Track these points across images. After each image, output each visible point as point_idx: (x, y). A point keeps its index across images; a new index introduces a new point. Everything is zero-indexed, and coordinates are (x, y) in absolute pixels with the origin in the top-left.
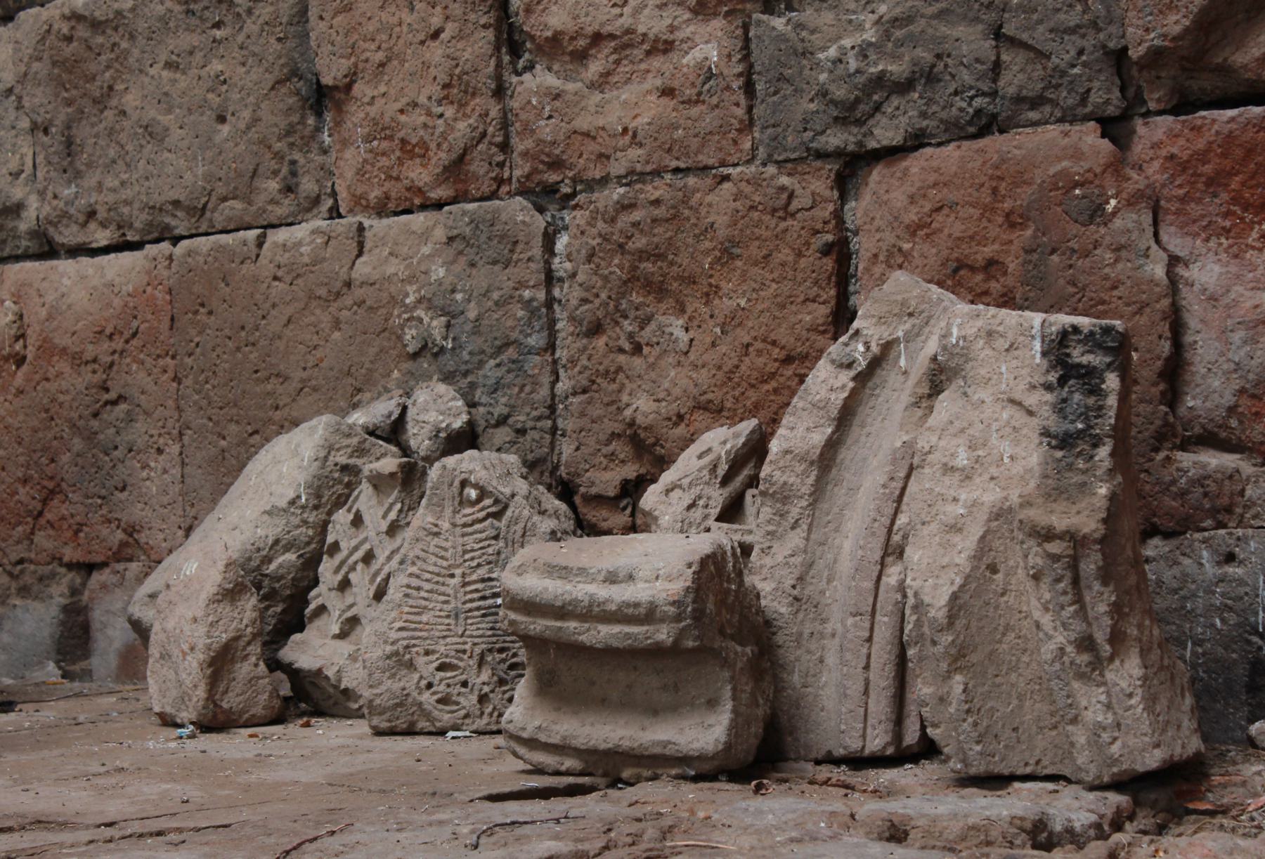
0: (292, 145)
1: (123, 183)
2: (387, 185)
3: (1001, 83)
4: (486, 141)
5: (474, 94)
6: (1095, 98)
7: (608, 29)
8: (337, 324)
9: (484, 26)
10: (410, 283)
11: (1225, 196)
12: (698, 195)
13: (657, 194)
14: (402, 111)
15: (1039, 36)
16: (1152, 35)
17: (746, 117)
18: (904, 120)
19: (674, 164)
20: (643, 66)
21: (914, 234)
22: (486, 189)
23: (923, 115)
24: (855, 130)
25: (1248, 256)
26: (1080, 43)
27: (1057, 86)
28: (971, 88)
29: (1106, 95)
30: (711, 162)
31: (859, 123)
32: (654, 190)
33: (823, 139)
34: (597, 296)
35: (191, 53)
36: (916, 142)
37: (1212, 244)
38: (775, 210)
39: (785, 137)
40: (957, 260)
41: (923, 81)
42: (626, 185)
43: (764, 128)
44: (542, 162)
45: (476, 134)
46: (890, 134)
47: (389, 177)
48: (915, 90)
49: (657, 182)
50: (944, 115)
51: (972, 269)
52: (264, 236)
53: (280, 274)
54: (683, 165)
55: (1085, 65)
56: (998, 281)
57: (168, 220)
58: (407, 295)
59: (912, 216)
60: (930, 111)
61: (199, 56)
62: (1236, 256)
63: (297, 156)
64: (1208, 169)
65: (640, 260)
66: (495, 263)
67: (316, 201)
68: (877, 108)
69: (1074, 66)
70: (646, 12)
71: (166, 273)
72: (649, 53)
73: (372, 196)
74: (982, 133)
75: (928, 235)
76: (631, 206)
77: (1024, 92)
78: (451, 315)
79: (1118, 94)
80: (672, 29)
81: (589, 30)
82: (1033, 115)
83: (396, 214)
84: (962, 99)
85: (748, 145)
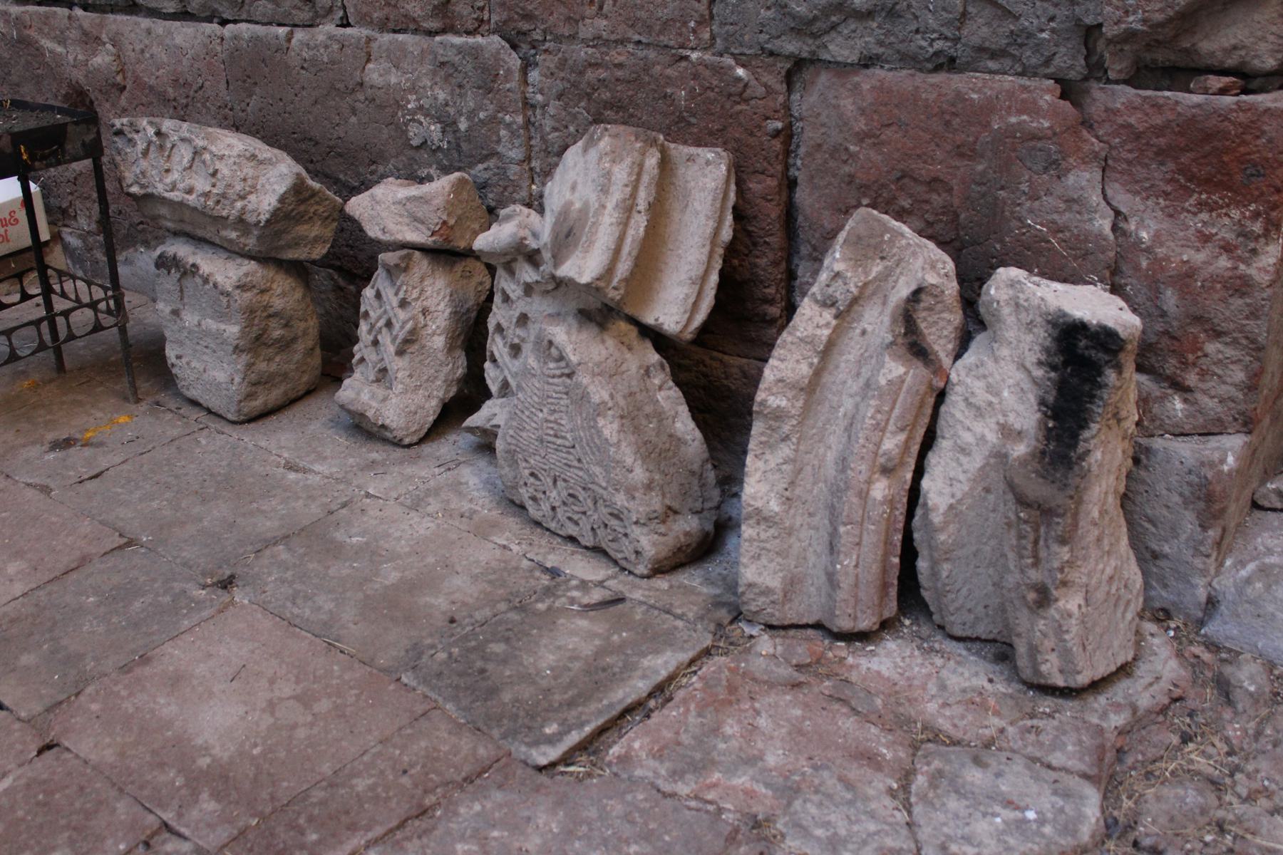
2: (387, 10)
3: (965, 32)
6: (1057, 61)
8: (354, 111)
10: (410, 93)
11: (1171, 165)
12: (658, 68)
13: (621, 59)
16: (1131, 19)
17: (706, 13)
18: (859, 43)
19: (637, 37)
21: (862, 140)
22: (470, 25)
23: (881, 43)
24: (810, 41)
25: (1182, 217)
27: (1021, 46)
28: (934, 31)
29: (1069, 60)
30: (672, 43)
31: (814, 36)
32: (617, 55)
33: (778, 42)
34: (566, 127)
36: (867, 62)
37: (1149, 203)
38: (730, 95)
39: (742, 35)
40: (903, 171)
41: (883, 14)
42: (593, 47)
43: (723, 24)
44: (517, 13)
46: (846, 53)
48: (873, 20)
49: (620, 49)
50: (902, 47)
52: (292, 33)
54: (644, 40)
55: (1053, 31)
56: (939, 195)
58: (409, 102)
59: (861, 125)
60: (887, 41)
62: (1171, 216)
64: (1162, 141)
65: (605, 108)
66: (479, 88)
67: (330, 10)
68: (834, 27)
69: (1042, 31)
71: (219, 48)
73: (375, 15)
74: (937, 69)
75: (874, 144)
76: (596, 65)
77: (987, 44)
78: (448, 125)
79: (1083, 62)
82: (992, 65)
83: (395, 32)
84: (923, 39)
85: (707, 36)
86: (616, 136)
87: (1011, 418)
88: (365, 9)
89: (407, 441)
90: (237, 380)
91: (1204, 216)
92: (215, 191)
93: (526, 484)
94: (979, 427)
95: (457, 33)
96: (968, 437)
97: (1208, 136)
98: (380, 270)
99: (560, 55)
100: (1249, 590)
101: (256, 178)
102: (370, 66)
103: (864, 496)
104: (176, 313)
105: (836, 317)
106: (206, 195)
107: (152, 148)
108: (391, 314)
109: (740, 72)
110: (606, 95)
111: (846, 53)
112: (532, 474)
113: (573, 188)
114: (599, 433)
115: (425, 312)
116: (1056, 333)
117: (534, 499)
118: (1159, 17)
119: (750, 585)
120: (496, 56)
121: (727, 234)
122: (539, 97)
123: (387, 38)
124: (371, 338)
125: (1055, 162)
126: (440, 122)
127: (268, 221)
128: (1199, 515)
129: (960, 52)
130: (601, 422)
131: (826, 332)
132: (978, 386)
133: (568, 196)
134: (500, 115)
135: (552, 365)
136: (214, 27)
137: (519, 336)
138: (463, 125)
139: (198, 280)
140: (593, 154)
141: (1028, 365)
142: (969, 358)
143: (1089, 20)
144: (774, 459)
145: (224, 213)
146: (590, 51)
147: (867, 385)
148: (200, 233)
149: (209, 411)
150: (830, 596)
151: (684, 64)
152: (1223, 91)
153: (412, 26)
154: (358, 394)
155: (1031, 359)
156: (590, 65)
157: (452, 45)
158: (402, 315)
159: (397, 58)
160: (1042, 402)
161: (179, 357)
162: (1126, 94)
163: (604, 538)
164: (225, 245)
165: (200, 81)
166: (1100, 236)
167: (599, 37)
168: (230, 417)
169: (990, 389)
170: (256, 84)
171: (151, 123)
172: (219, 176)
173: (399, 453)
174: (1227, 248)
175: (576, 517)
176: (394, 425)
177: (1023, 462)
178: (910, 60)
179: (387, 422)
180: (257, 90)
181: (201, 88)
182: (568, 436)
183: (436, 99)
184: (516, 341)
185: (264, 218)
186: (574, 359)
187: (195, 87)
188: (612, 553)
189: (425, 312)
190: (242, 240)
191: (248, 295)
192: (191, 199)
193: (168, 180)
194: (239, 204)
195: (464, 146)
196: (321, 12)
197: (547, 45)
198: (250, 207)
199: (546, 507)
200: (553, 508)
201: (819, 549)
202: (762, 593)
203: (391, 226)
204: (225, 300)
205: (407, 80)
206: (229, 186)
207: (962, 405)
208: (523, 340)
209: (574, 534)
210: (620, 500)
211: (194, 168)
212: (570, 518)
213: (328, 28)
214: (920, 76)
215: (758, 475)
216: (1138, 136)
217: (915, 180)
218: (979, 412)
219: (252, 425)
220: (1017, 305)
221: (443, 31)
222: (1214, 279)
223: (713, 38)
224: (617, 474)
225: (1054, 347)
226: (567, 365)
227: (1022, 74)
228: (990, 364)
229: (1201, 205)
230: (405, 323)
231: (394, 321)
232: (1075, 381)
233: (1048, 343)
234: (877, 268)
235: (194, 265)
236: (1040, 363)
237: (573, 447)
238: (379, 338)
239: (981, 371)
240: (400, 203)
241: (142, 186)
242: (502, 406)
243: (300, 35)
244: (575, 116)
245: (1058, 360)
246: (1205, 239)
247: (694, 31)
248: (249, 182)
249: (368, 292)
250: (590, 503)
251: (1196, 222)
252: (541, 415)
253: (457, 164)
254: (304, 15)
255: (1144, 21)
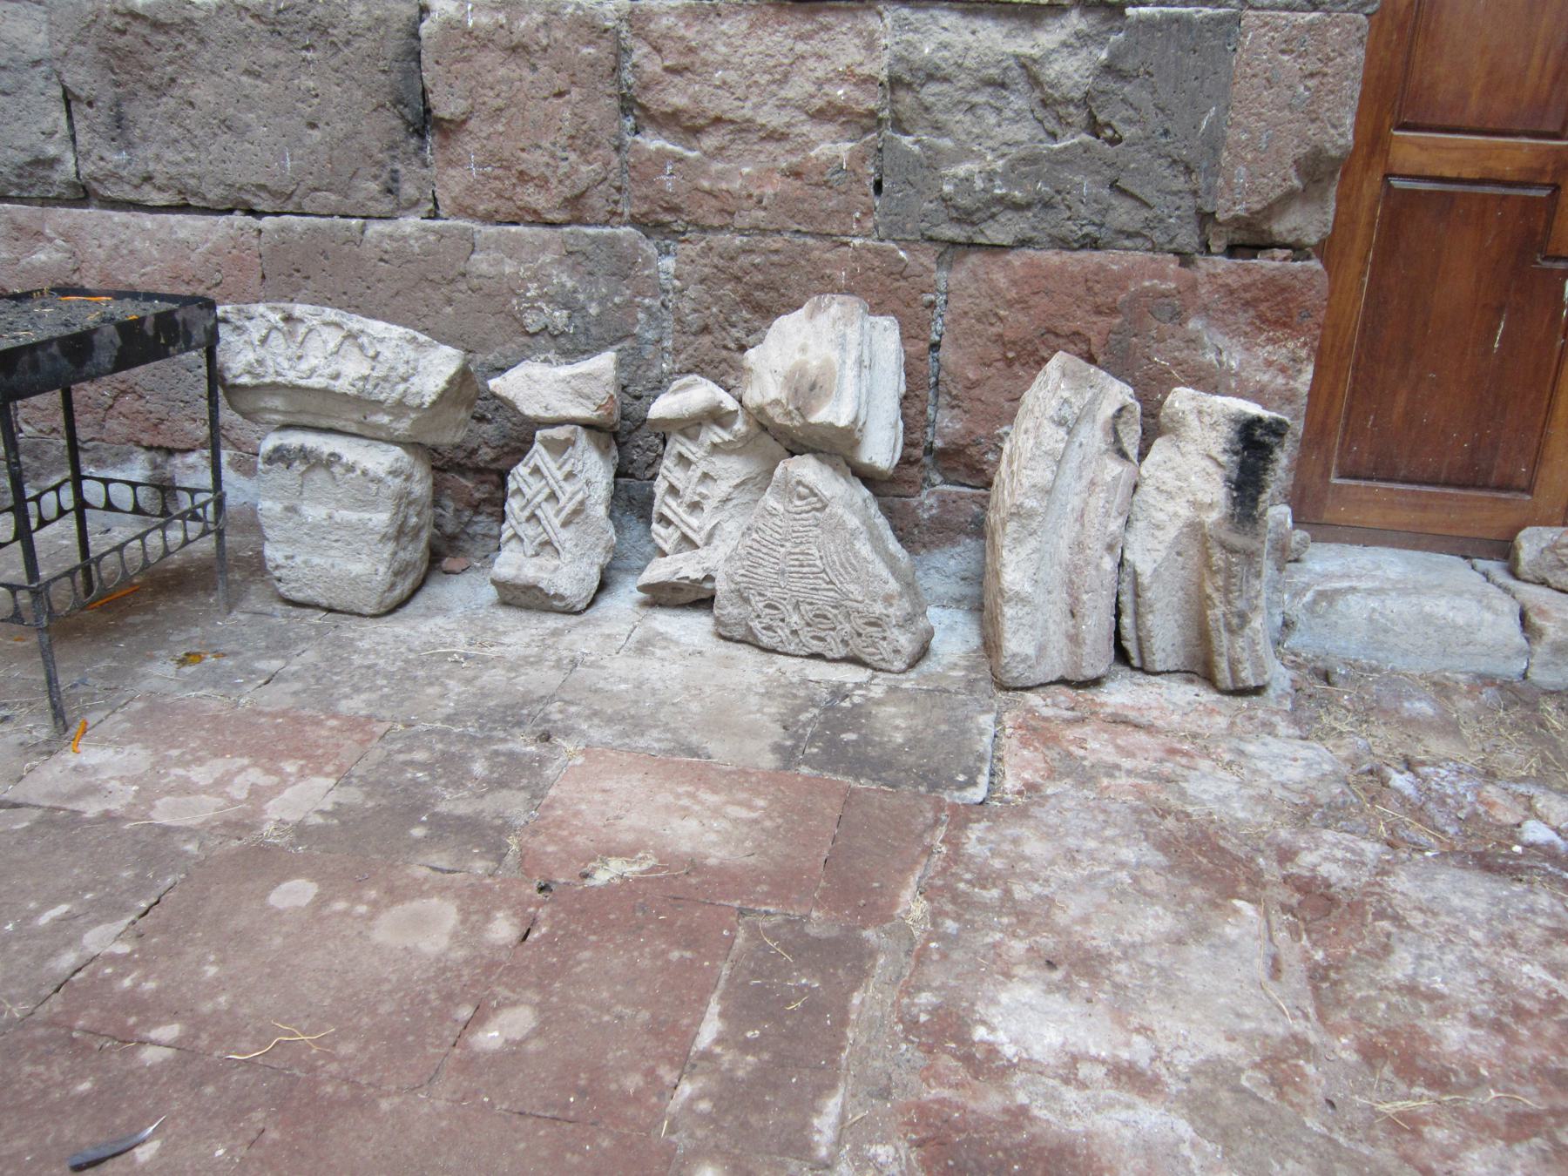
0: (394, 157)
1: (188, 160)
2: (497, 202)
3: (1108, 219)
4: (606, 184)
5: (597, 147)
6: (1179, 239)
7: (730, 116)
8: (450, 302)
9: (610, 96)
11: (1252, 312)
12: (817, 253)
14: (523, 150)
15: (1147, 193)
19: (796, 227)
20: (756, 147)
23: (1034, 229)
26: (1178, 202)
29: (1187, 238)
31: (973, 224)
33: (937, 230)
35: (276, 66)
36: (1024, 243)
45: (599, 178)
47: (500, 196)
49: (777, 237)
50: (1054, 232)
51: (1057, 335)
53: (386, 257)
54: (803, 229)
55: (1178, 217)
57: (247, 197)
58: (528, 290)
59: (1013, 294)
61: (284, 71)
63: (398, 166)
64: (1248, 296)
68: (993, 216)
70: (765, 108)
71: (255, 242)
72: (762, 139)
73: (481, 207)
74: (1082, 247)
80: (789, 125)
81: (712, 114)
82: (1127, 243)
85: (870, 225)
86: (843, 304)
87: (1200, 496)
88: (468, 201)
89: (579, 607)
90: (382, 569)
91: (1269, 348)
92: (375, 374)
93: (758, 616)
94: (1170, 507)
95: (588, 224)
96: (1161, 516)
97: (1283, 290)
98: (537, 446)
99: (703, 244)
100: (1318, 608)
101: (416, 360)
102: (474, 257)
103: (1098, 567)
104: (292, 509)
105: (1068, 433)
106: (365, 378)
107: (274, 334)
108: (556, 487)
109: (902, 254)
110: (759, 278)
111: (1002, 237)
112: (769, 606)
113: (803, 349)
114: (856, 555)
115: (588, 483)
116: (1238, 427)
117: (769, 628)
118: (1258, 207)
119: (1014, 655)
120: (634, 246)
121: (903, 389)
122: (677, 283)
123: (492, 230)
124: (527, 513)
125: (1179, 313)
126: (567, 308)
127: (434, 403)
128: (1276, 562)
129: (1105, 235)
130: (858, 545)
131: (1062, 445)
132: (1168, 477)
133: (798, 357)
134: (638, 299)
135: (798, 503)
136: (239, 219)
137: (700, 494)
138: (594, 310)
139: (337, 470)
140: (823, 320)
141: (1214, 454)
142: (1155, 455)
143: (1208, 209)
144: (1024, 551)
145: (382, 397)
146: (745, 239)
147: (1092, 483)
148: (324, 423)
149: (330, 610)
150: (1072, 653)
151: (845, 249)
152: (1285, 259)
153: (529, 218)
154: (520, 568)
155: (1216, 451)
156: (744, 251)
157: (587, 236)
158: (569, 488)
159: (514, 249)
160: (1228, 480)
161: (287, 558)
162: (1222, 263)
163: (858, 647)
164: (367, 433)
165: (218, 276)
166: (1211, 364)
167: (757, 228)
168: (367, 610)
169: (1178, 477)
170: (308, 278)
171: (274, 309)
172: (381, 358)
173: (574, 619)
174: (1283, 370)
175: (822, 634)
176: (568, 593)
177: (1217, 524)
178: (1063, 244)
179: (561, 591)
180: (310, 284)
181: (217, 285)
182: (818, 562)
183: (563, 286)
184: (697, 498)
185: (428, 400)
186: (827, 494)
187: (208, 283)
188: (868, 659)
189: (588, 483)
190: (394, 425)
191: (397, 481)
192: (341, 386)
193: (304, 366)
194: (401, 387)
195: (594, 331)
196: (405, 204)
197: (688, 236)
198: (414, 389)
199: (784, 633)
200: (795, 632)
201: (1058, 619)
202: (1023, 661)
203: (554, 403)
204: (374, 487)
205: (526, 270)
206: (392, 368)
207: (1154, 493)
208: (705, 497)
209: (819, 650)
210: (878, 608)
211: (342, 352)
212: (813, 638)
213: (410, 223)
214: (1066, 254)
215: (1012, 566)
216: (1232, 292)
217: (1057, 335)
218: (1170, 496)
219: (389, 618)
220: (1200, 412)
221: (568, 223)
222: (1277, 392)
223: (876, 227)
224: (876, 586)
225: (1236, 438)
226: (820, 500)
227: (1153, 250)
228: (1178, 459)
229: (1270, 340)
230: (575, 494)
231: (559, 493)
232: (1251, 460)
233: (1232, 435)
234: (1088, 394)
235: (332, 455)
236: (1225, 451)
237: (824, 571)
238: (538, 512)
239: (1169, 465)
240: (563, 380)
241: (258, 376)
242: (685, 560)
243: (376, 227)
244: (720, 298)
245: (1239, 447)
246: (1269, 364)
247: (858, 221)
248: (412, 364)
249: (522, 470)
250: (840, 617)
251: (1263, 353)
252: (782, 550)
253: (582, 348)
254: (386, 206)
255: (1247, 210)
